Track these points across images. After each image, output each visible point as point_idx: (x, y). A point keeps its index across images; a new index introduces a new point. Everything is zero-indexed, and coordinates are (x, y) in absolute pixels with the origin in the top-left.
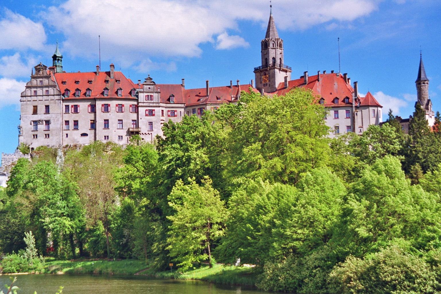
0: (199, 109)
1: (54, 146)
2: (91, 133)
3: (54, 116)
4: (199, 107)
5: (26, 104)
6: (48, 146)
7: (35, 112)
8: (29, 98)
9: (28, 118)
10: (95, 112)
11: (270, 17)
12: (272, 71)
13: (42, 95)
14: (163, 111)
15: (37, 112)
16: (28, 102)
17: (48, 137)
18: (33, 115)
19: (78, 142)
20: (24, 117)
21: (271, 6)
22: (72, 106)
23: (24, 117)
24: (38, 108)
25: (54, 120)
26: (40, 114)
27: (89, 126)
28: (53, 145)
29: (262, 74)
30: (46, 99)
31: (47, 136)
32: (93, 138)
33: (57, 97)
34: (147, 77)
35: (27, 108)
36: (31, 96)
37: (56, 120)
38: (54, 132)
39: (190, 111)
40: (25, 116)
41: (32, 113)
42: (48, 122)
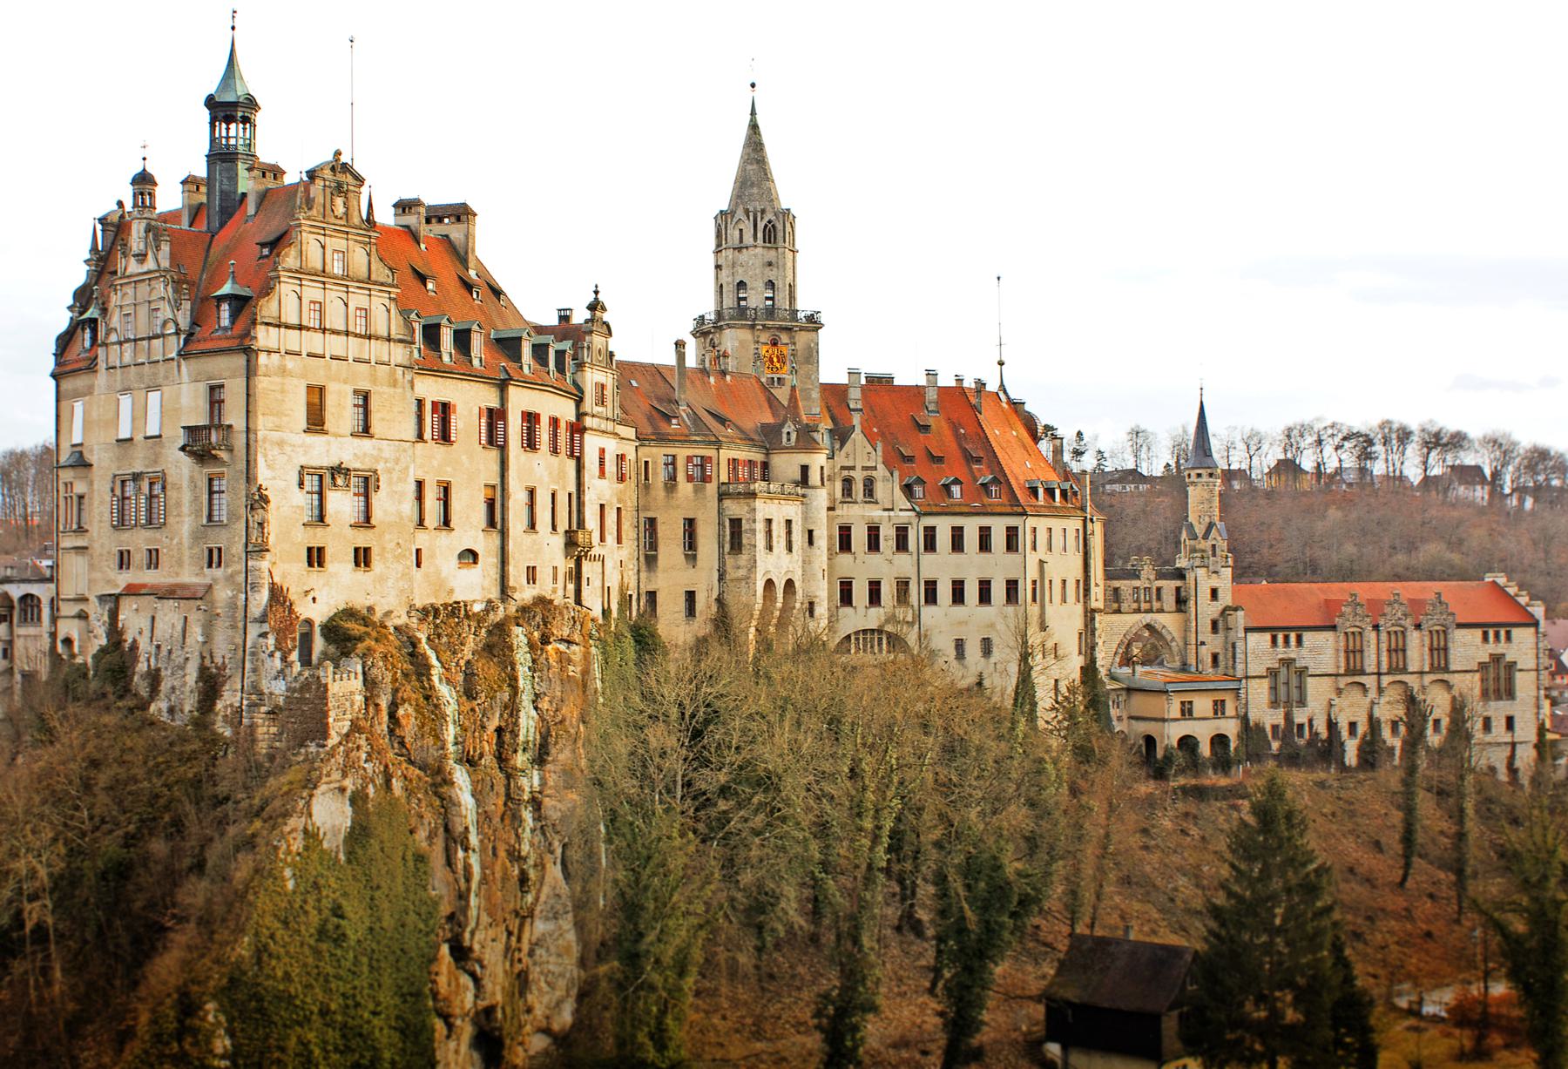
0: (689, 459)
1: (388, 614)
2: (487, 545)
3: (388, 449)
4: (690, 452)
5: (283, 371)
6: (371, 609)
7: (316, 421)
8: (292, 339)
9: (288, 449)
10: (503, 449)
12: (802, 338)
13: (342, 328)
14: (602, 451)
15: (323, 424)
16: (290, 362)
17: (367, 564)
19: (451, 591)
21: (753, 85)
22: (434, 403)
25: (389, 471)
26: (337, 435)
28: (387, 608)
29: (762, 340)
31: (362, 557)
32: (494, 573)
33: (399, 354)
35: (282, 392)
36: (300, 328)
38: (389, 540)
39: (655, 463)
40: (275, 435)
41: (304, 425)
42: (368, 486)
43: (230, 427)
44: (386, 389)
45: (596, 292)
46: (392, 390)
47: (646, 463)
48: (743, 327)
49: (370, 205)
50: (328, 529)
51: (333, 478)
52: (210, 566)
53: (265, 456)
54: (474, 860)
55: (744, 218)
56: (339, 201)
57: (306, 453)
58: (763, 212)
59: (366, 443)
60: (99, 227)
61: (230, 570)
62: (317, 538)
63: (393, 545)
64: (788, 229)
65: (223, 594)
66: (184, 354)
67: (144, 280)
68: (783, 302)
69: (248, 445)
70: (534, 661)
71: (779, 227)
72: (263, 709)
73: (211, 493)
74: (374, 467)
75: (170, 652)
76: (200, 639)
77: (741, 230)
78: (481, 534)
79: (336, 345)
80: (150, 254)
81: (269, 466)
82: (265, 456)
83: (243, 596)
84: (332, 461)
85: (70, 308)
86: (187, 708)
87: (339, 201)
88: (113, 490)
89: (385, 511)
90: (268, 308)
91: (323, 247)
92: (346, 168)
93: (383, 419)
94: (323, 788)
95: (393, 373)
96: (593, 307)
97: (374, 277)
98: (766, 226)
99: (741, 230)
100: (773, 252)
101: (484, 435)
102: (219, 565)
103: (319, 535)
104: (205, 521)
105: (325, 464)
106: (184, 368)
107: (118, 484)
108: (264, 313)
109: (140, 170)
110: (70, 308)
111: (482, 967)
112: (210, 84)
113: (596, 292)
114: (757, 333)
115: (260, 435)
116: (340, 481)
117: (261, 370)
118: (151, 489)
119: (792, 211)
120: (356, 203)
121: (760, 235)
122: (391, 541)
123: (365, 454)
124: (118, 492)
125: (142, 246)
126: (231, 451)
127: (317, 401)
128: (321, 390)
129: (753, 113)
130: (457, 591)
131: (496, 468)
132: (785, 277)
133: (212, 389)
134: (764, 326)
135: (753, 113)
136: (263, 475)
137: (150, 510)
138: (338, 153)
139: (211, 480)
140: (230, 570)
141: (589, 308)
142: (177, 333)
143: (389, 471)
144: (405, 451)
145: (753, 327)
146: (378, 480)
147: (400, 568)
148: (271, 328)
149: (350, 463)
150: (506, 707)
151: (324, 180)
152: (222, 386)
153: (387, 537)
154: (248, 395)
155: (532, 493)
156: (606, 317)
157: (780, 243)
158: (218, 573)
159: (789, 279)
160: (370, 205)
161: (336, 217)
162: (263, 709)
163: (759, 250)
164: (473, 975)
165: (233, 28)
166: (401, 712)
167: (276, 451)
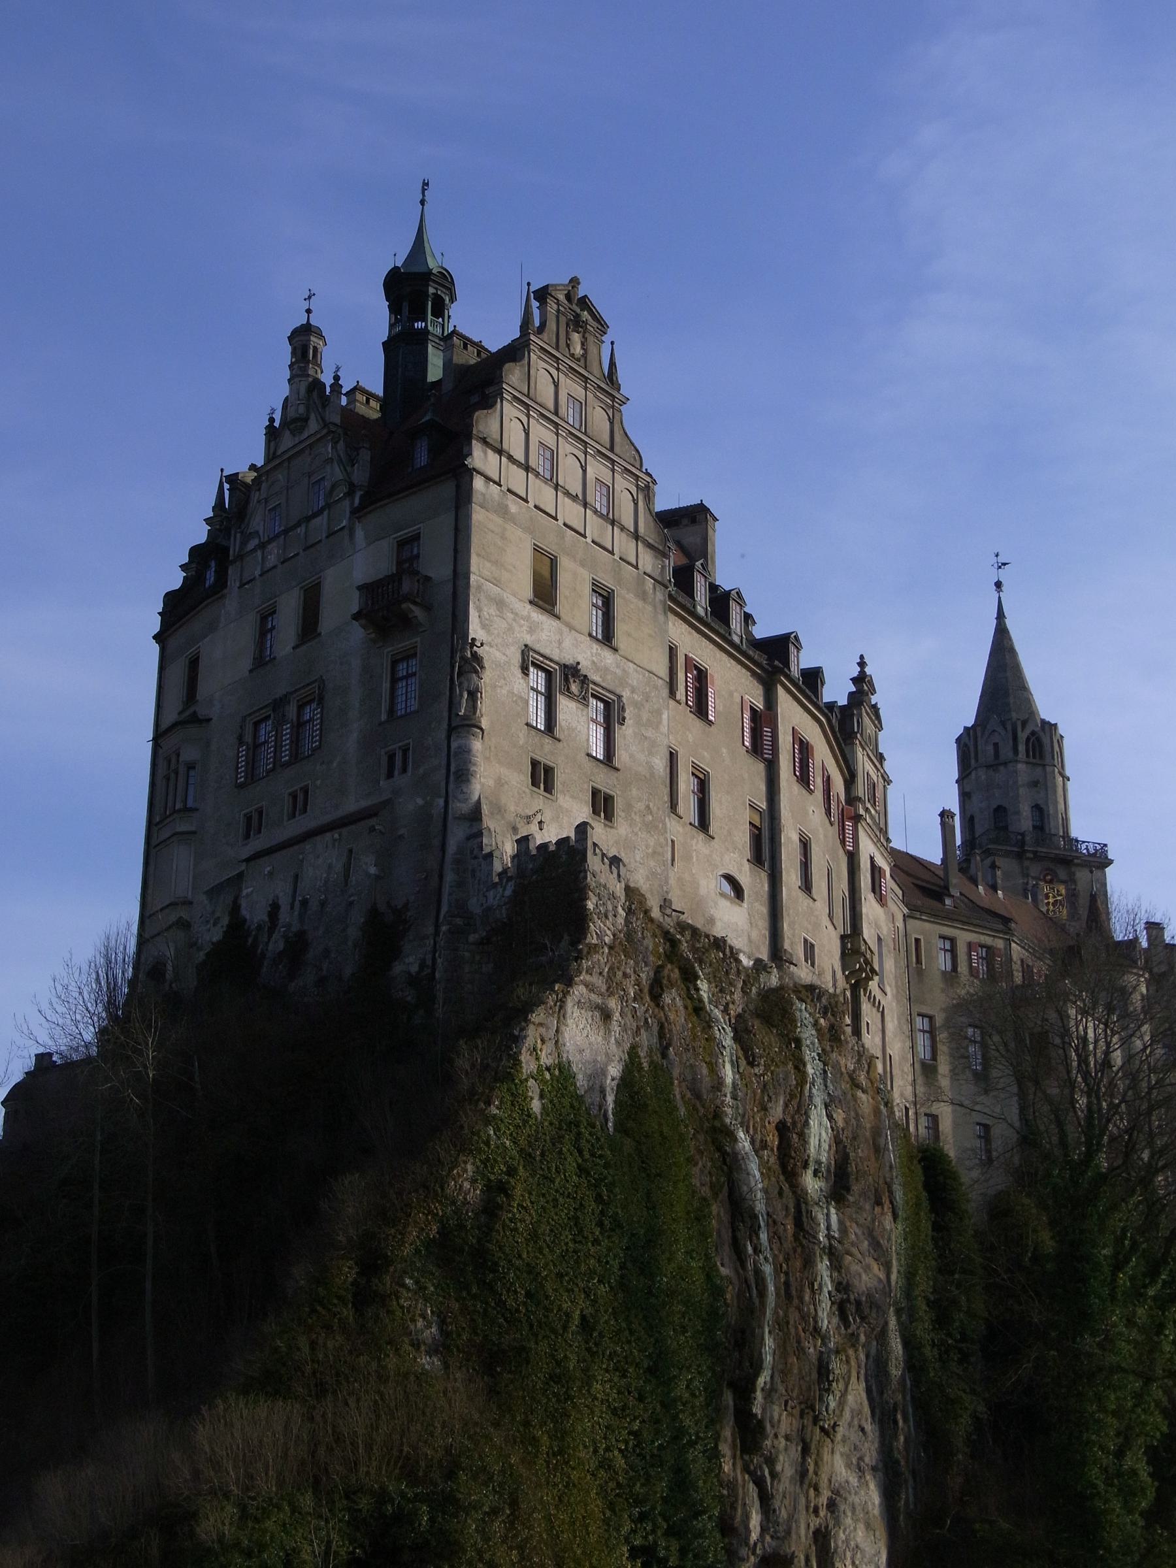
2: (753, 880)
5: (503, 511)
8: (516, 478)
11: (1001, 634)
12: (1082, 875)
15: (554, 604)
16: (514, 506)
18: (537, 616)
19: (711, 921)
20: (491, 599)
21: (998, 585)
23: (491, 599)
24: (564, 579)
25: (638, 706)
26: (571, 628)
27: (743, 838)
30: (597, 540)
33: (647, 561)
34: (855, 671)
35: (503, 538)
37: (645, 716)
39: (928, 942)
41: (528, 593)
43: (428, 579)
44: (630, 596)
45: (862, 664)
46: (640, 604)
47: (917, 941)
48: (1007, 854)
49: (612, 364)
50: (560, 745)
51: (567, 680)
52: (390, 775)
53: (479, 610)
54: (768, 1269)
55: (1000, 729)
56: (576, 337)
57: (531, 631)
58: (1024, 723)
59: (608, 657)
60: (227, 486)
61: (421, 771)
62: (546, 752)
63: (640, 806)
64: (1056, 748)
65: (410, 804)
66: (358, 513)
67: (302, 451)
68: (1055, 827)
69: (455, 594)
70: (823, 1050)
71: (1046, 740)
72: (472, 938)
73: (394, 681)
74: (618, 691)
75: (323, 904)
76: (373, 870)
77: (996, 745)
78: (747, 866)
79: (571, 512)
80: (312, 416)
81: (484, 626)
82: (479, 610)
83: (441, 802)
84: (569, 660)
85: (184, 567)
86: (348, 971)
87: (576, 337)
88: (240, 740)
89: (631, 756)
90: (486, 423)
91: (556, 385)
92: (584, 303)
93: (629, 635)
94: (579, 991)
95: (640, 583)
96: (861, 680)
97: (617, 449)
98: (1028, 739)
99: (996, 745)
100: (1039, 770)
101: (747, 734)
102: (404, 770)
103: (547, 748)
104: (384, 717)
105: (556, 658)
106: (359, 534)
107: (249, 728)
108: (481, 428)
109: (305, 322)
110: (184, 567)
111: (774, 1475)
112: (397, 254)
113: (862, 664)
114: (1027, 863)
115: (473, 578)
116: (574, 688)
117: (476, 498)
118: (299, 715)
119: (1061, 730)
120: (595, 351)
121: (1022, 748)
122: (640, 800)
123: (606, 669)
124: (248, 738)
125: (302, 409)
126: (428, 608)
127: (546, 573)
128: (553, 562)
129: (1001, 615)
130: (719, 924)
131: (763, 787)
132: (1056, 803)
133: (402, 544)
134: (1035, 853)
135: (1001, 615)
136: (475, 630)
137: (296, 741)
138: (575, 282)
139: (394, 663)
140: (421, 771)
141: (854, 680)
142: (350, 494)
143: (638, 706)
144: (656, 687)
145: (1020, 856)
146: (622, 709)
147: (652, 842)
148: (490, 452)
149: (585, 667)
150: (792, 1096)
151: (558, 303)
152: (416, 537)
153: (634, 792)
154: (457, 529)
155: (805, 845)
156: (874, 699)
157: (1048, 760)
158: (400, 780)
159: (1061, 806)
160: (612, 364)
161: (573, 355)
162: (472, 938)
163: (1020, 766)
164: (759, 1483)
165: (422, 202)
166: (667, 999)
167: (493, 610)
